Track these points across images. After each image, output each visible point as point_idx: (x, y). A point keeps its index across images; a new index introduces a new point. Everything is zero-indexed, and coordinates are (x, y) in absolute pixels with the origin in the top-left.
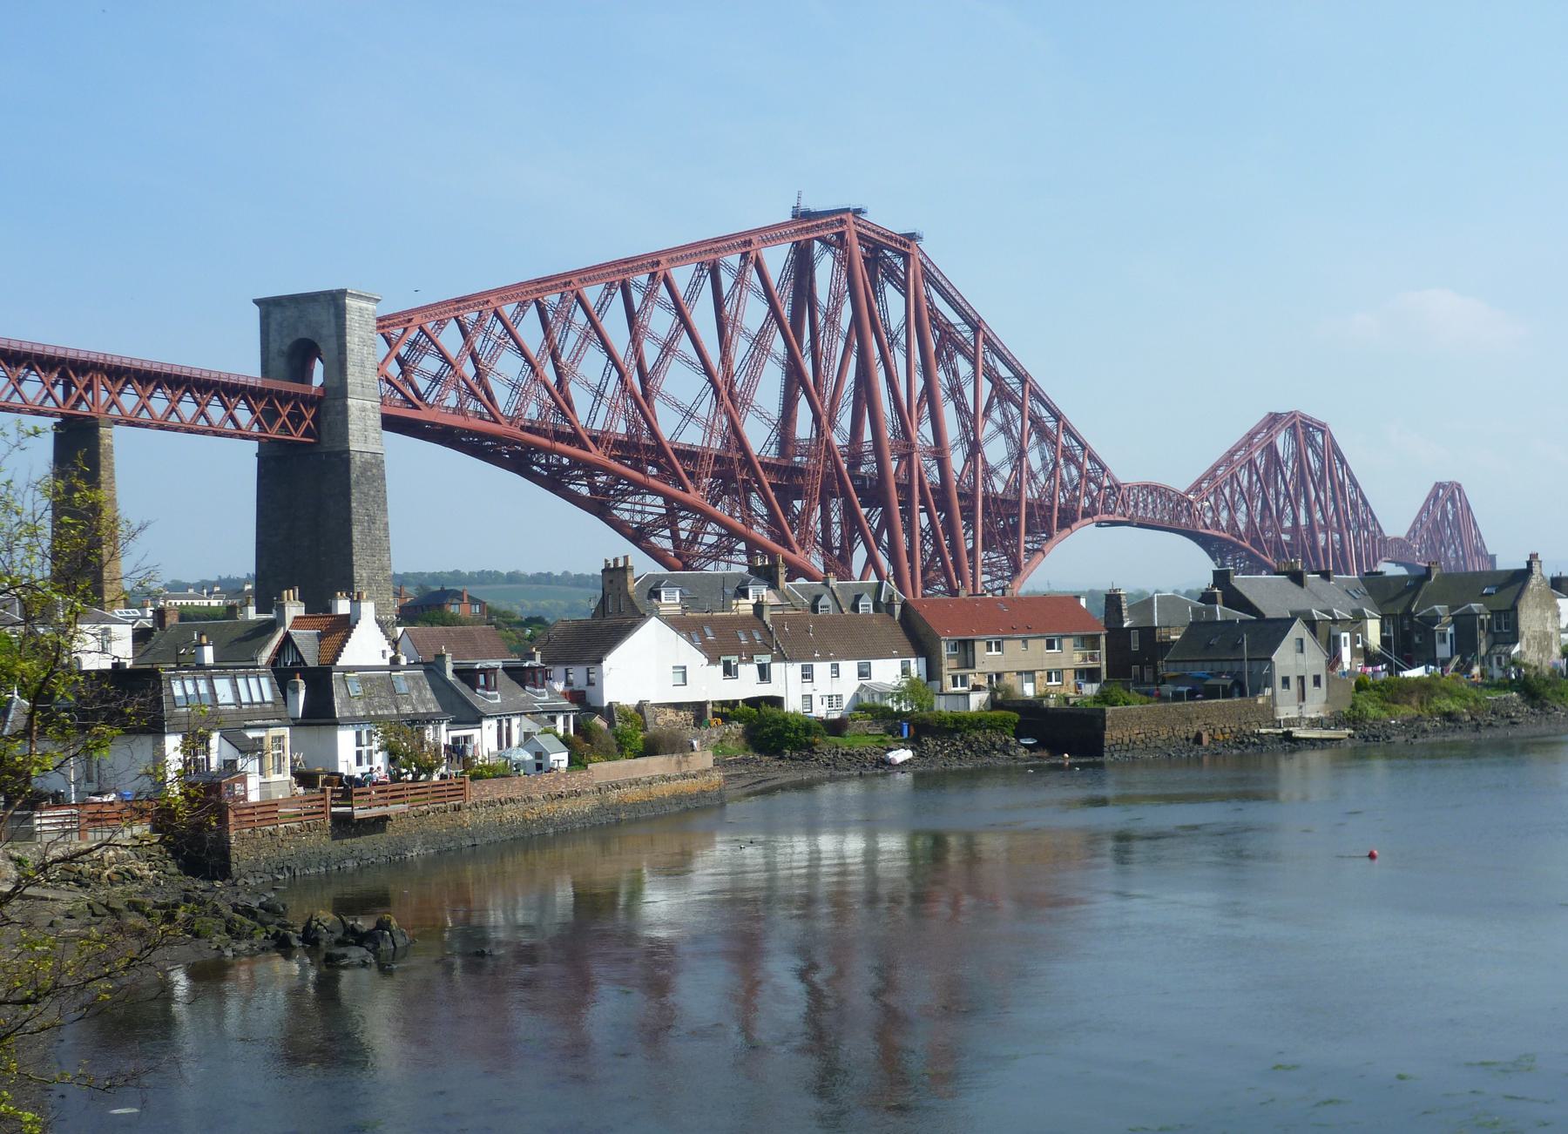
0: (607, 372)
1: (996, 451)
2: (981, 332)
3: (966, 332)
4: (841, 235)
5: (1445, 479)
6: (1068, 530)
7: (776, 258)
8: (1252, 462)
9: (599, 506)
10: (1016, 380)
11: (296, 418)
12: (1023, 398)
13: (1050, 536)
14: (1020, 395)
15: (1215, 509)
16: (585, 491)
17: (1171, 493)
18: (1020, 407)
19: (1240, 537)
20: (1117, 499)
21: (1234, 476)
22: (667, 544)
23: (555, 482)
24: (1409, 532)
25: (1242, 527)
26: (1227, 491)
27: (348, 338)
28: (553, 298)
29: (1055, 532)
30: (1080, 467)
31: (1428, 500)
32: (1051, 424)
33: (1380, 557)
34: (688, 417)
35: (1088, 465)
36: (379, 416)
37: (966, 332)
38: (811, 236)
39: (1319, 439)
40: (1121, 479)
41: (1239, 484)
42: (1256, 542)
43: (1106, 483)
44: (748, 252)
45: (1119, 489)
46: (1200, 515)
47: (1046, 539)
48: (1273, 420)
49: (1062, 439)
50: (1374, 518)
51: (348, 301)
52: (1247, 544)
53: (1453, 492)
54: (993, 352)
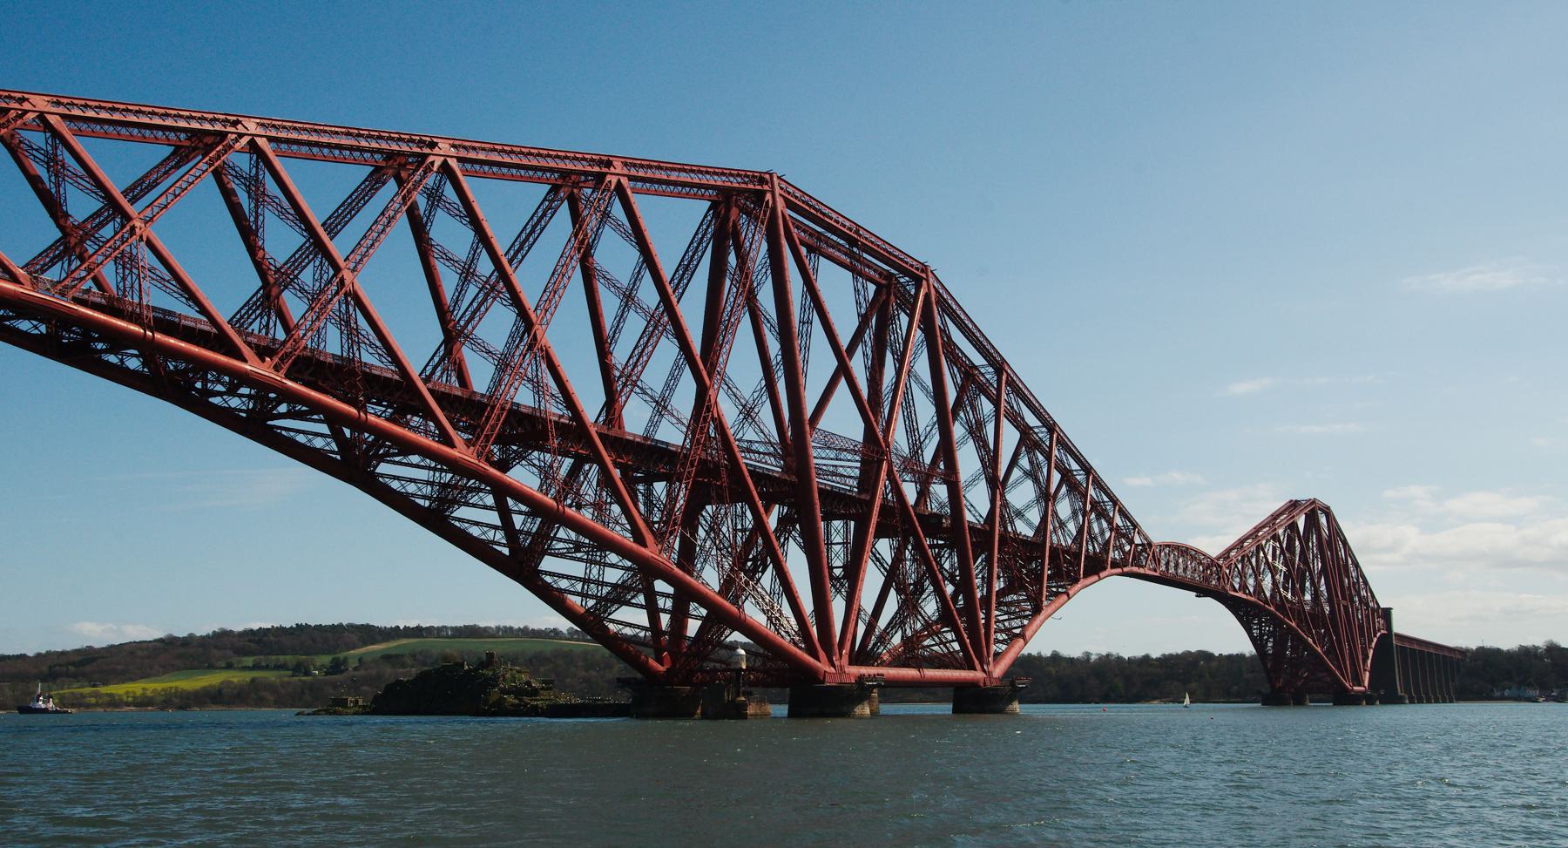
1: (1021, 494)
8: (1275, 538)
14: (1048, 443)
15: (1242, 575)
18: (1048, 457)
19: (1266, 602)
20: (1149, 555)
21: (1260, 548)
25: (1268, 594)
26: (1254, 560)
30: (1110, 521)
32: (1080, 477)
35: (1118, 520)
40: (1156, 538)
48: (1294, 505)
49: (1091, 491)
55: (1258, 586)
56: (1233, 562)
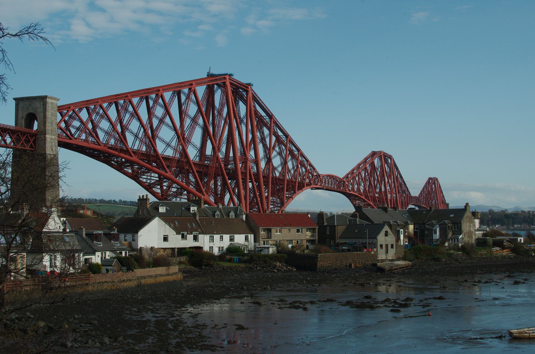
0: (140, 129)
1: (276, 161)
2: (273, 119)
3: (267, 119)
4: (224, 83)
5: (432, 176)
6: (301, 190)
7: (201, 90)
8: (366, 169)
9: (135, 177)
10: (284, 137)
11: (28, 141)
12: (287, 143)
13: (295, 192)
14: (286, 142)
15: (353, 185)
16: (130, 171)
17: (338, 178)
18: (285, 146)
19: (361, 195)
20: (319, 180)
21: (360, 173)
22: (159, 191)
23: (119, 168)
24: (420, 195)
25: (362, 191)
26: (357, 178)
27: (47, 113)
28: (122, 102)
29: (297, 191)
30: (306, 168)
31: (426, 183)
32: (296, 153)
33: (409, 203)
34: (168, 146)
35: (309, 168)
36: (57, 142)
37: (267, 119)
38: (214, 83)
39: (389, 161)
40: (320, 173)
41: (361, 176)
42: (366, 197)
43: (315, 174)
44: (191, 88)
45: (320, 176)
46: (347, 186)
47: (293, 193)
48: (374, 154)
49: (300, 158)
50: (408, 189)
51: (48, 100)
52: (363, 197)
53: (435, 181)
54: (277, 126)
55: (359, 189)
56: (349, 180)
